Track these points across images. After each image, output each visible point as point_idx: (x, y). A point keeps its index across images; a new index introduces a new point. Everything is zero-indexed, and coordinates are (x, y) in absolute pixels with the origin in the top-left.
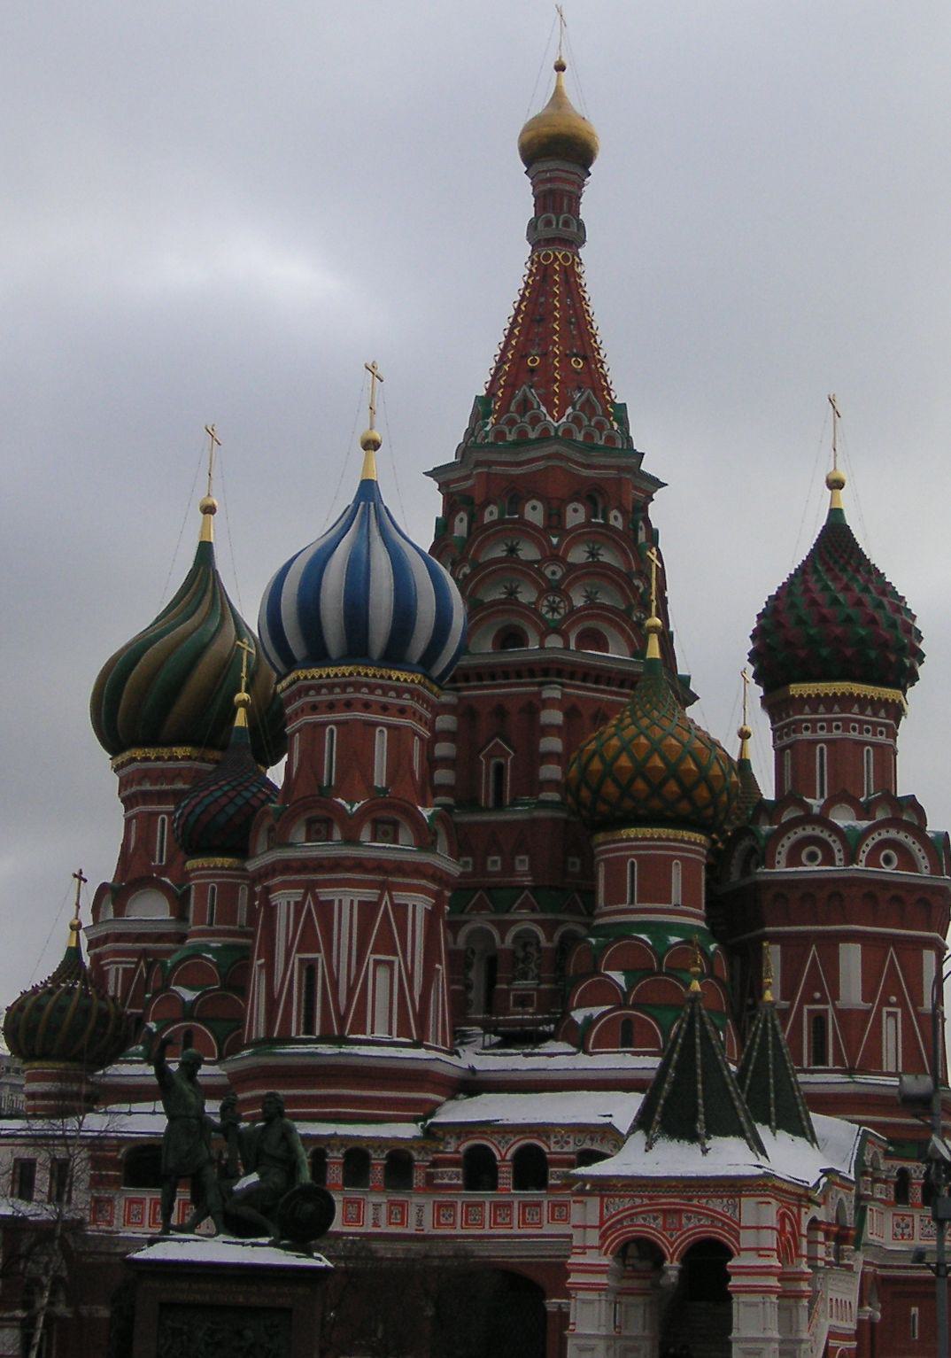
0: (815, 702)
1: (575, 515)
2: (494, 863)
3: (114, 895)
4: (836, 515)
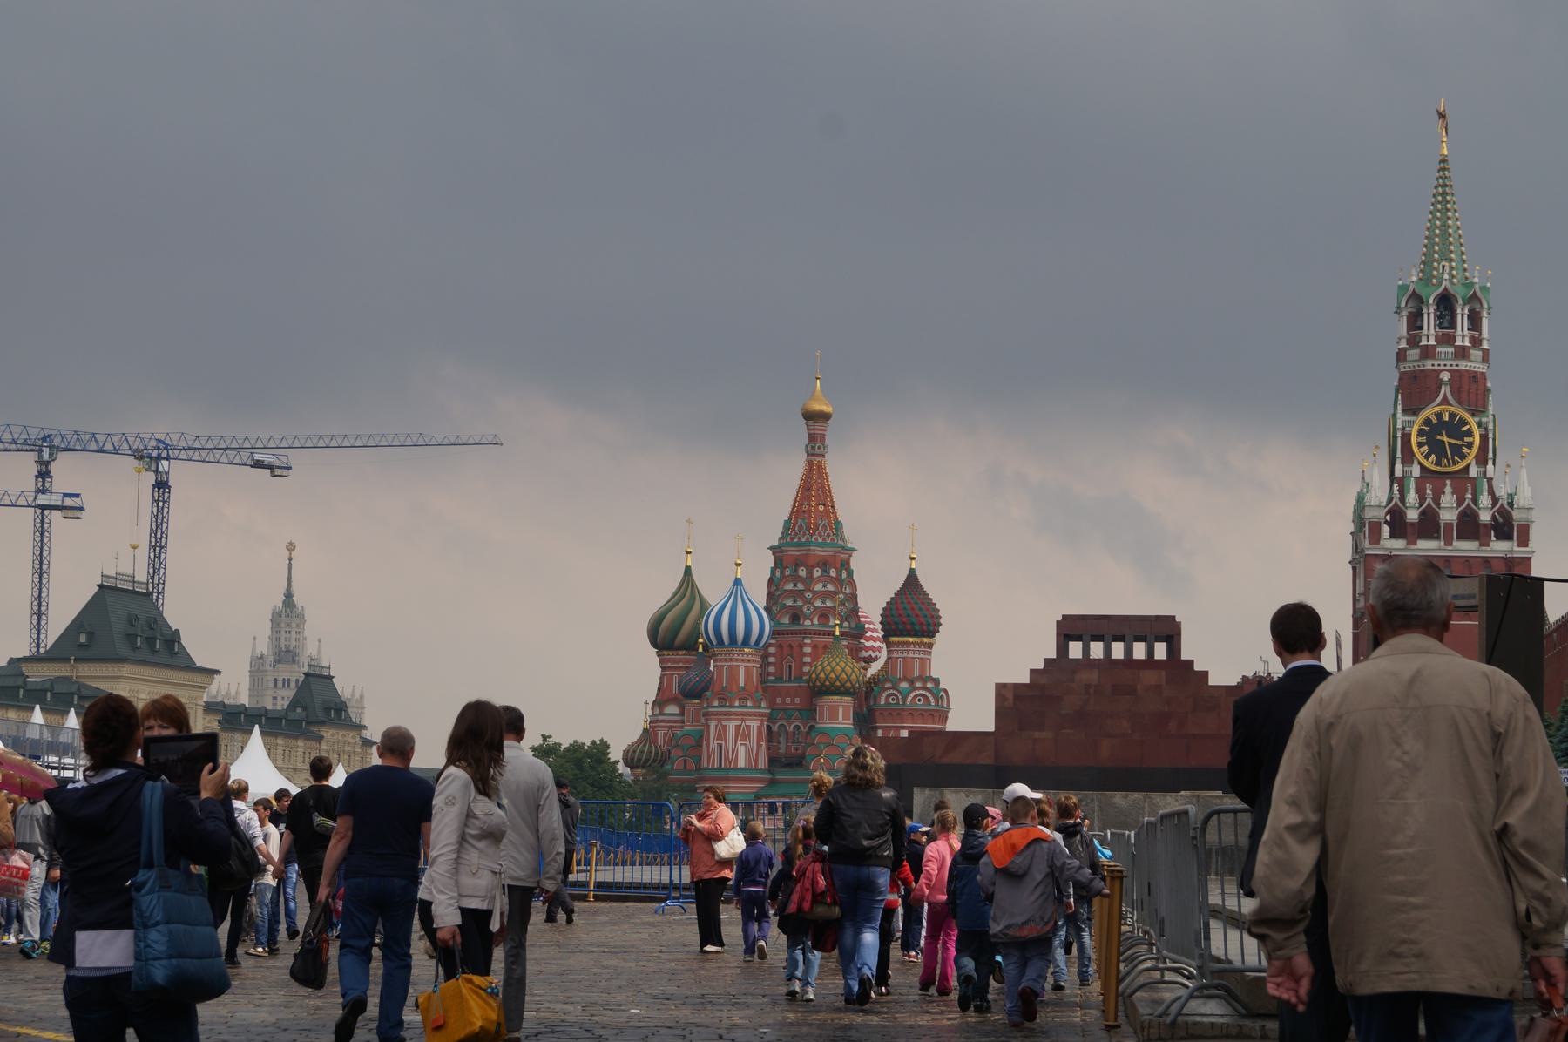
0: (898, 643)
1: (817, 573)
2: (788, 700)
3: (660, 702)
4: (912, 571)
